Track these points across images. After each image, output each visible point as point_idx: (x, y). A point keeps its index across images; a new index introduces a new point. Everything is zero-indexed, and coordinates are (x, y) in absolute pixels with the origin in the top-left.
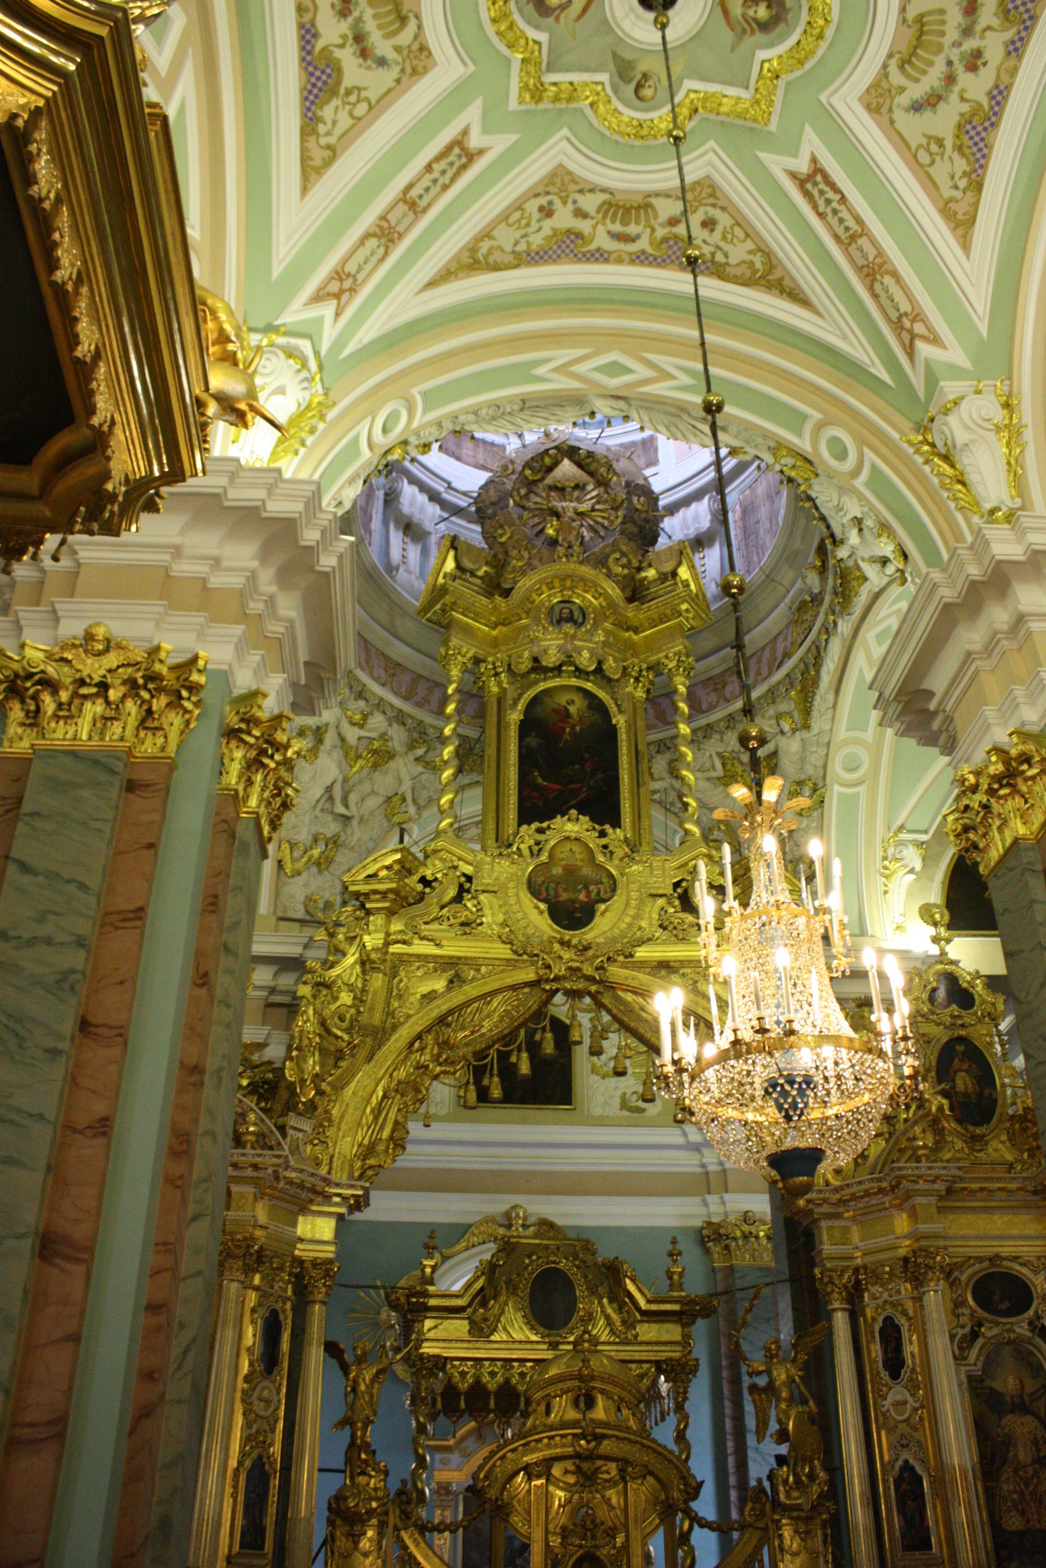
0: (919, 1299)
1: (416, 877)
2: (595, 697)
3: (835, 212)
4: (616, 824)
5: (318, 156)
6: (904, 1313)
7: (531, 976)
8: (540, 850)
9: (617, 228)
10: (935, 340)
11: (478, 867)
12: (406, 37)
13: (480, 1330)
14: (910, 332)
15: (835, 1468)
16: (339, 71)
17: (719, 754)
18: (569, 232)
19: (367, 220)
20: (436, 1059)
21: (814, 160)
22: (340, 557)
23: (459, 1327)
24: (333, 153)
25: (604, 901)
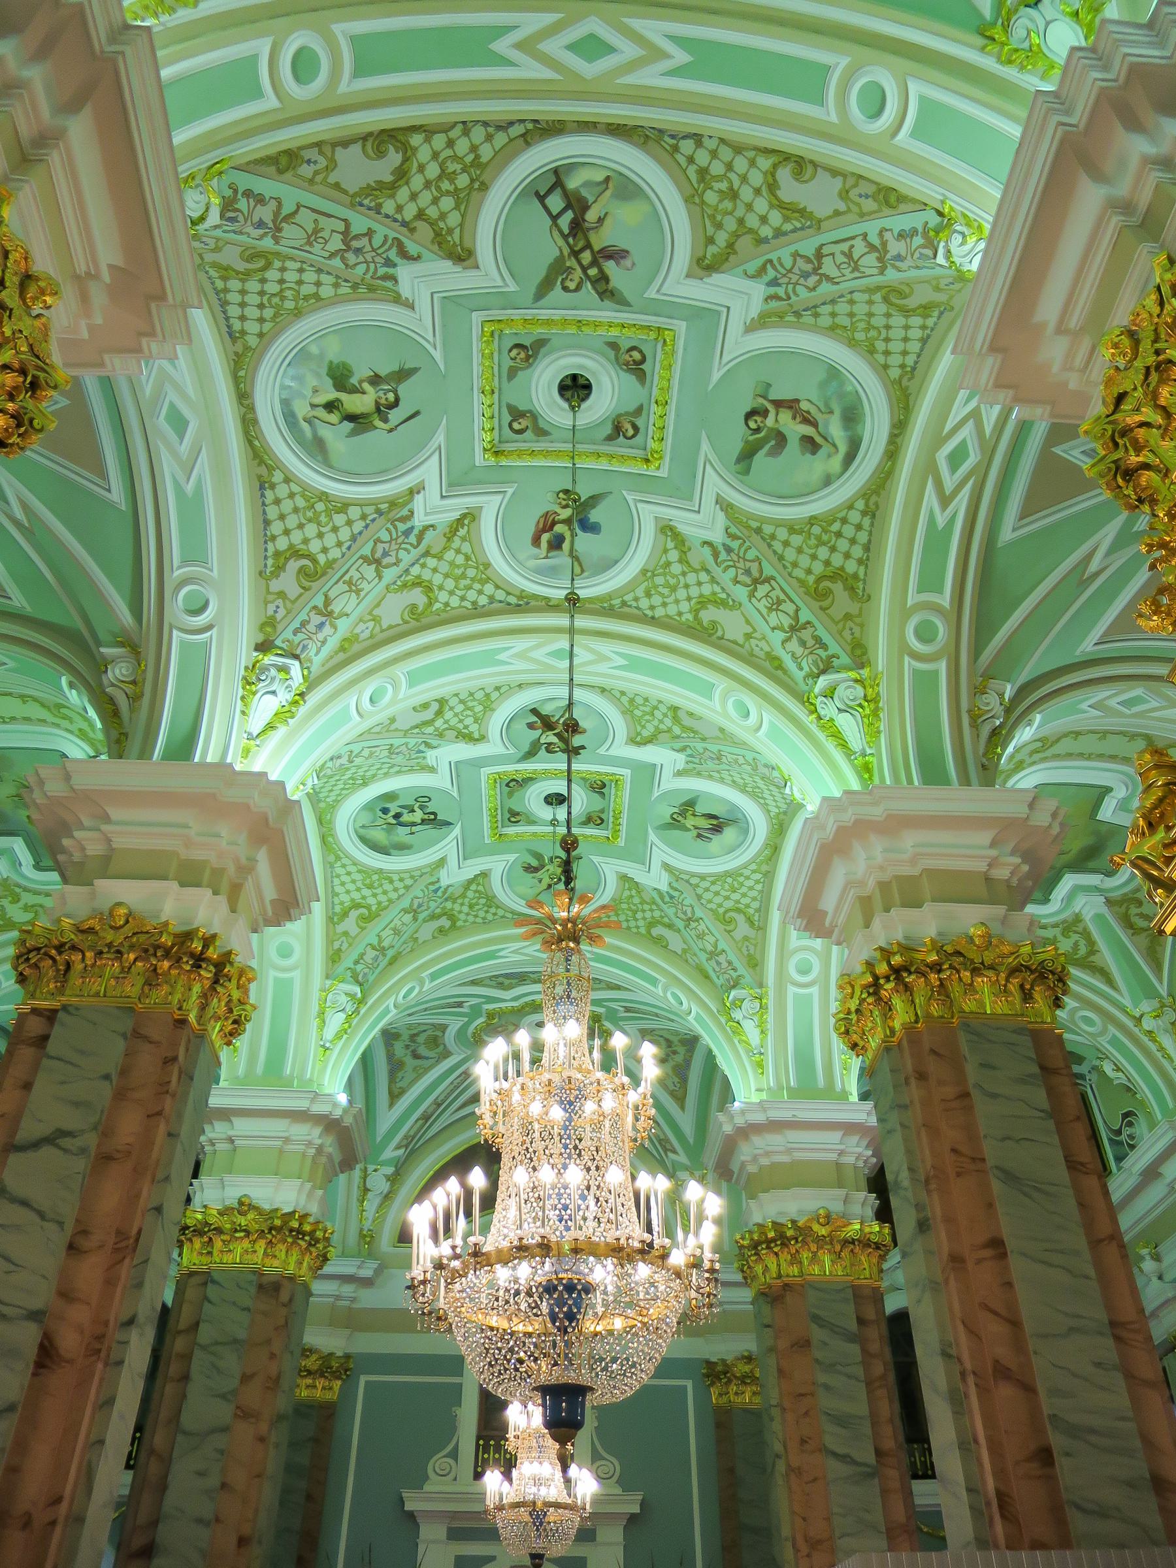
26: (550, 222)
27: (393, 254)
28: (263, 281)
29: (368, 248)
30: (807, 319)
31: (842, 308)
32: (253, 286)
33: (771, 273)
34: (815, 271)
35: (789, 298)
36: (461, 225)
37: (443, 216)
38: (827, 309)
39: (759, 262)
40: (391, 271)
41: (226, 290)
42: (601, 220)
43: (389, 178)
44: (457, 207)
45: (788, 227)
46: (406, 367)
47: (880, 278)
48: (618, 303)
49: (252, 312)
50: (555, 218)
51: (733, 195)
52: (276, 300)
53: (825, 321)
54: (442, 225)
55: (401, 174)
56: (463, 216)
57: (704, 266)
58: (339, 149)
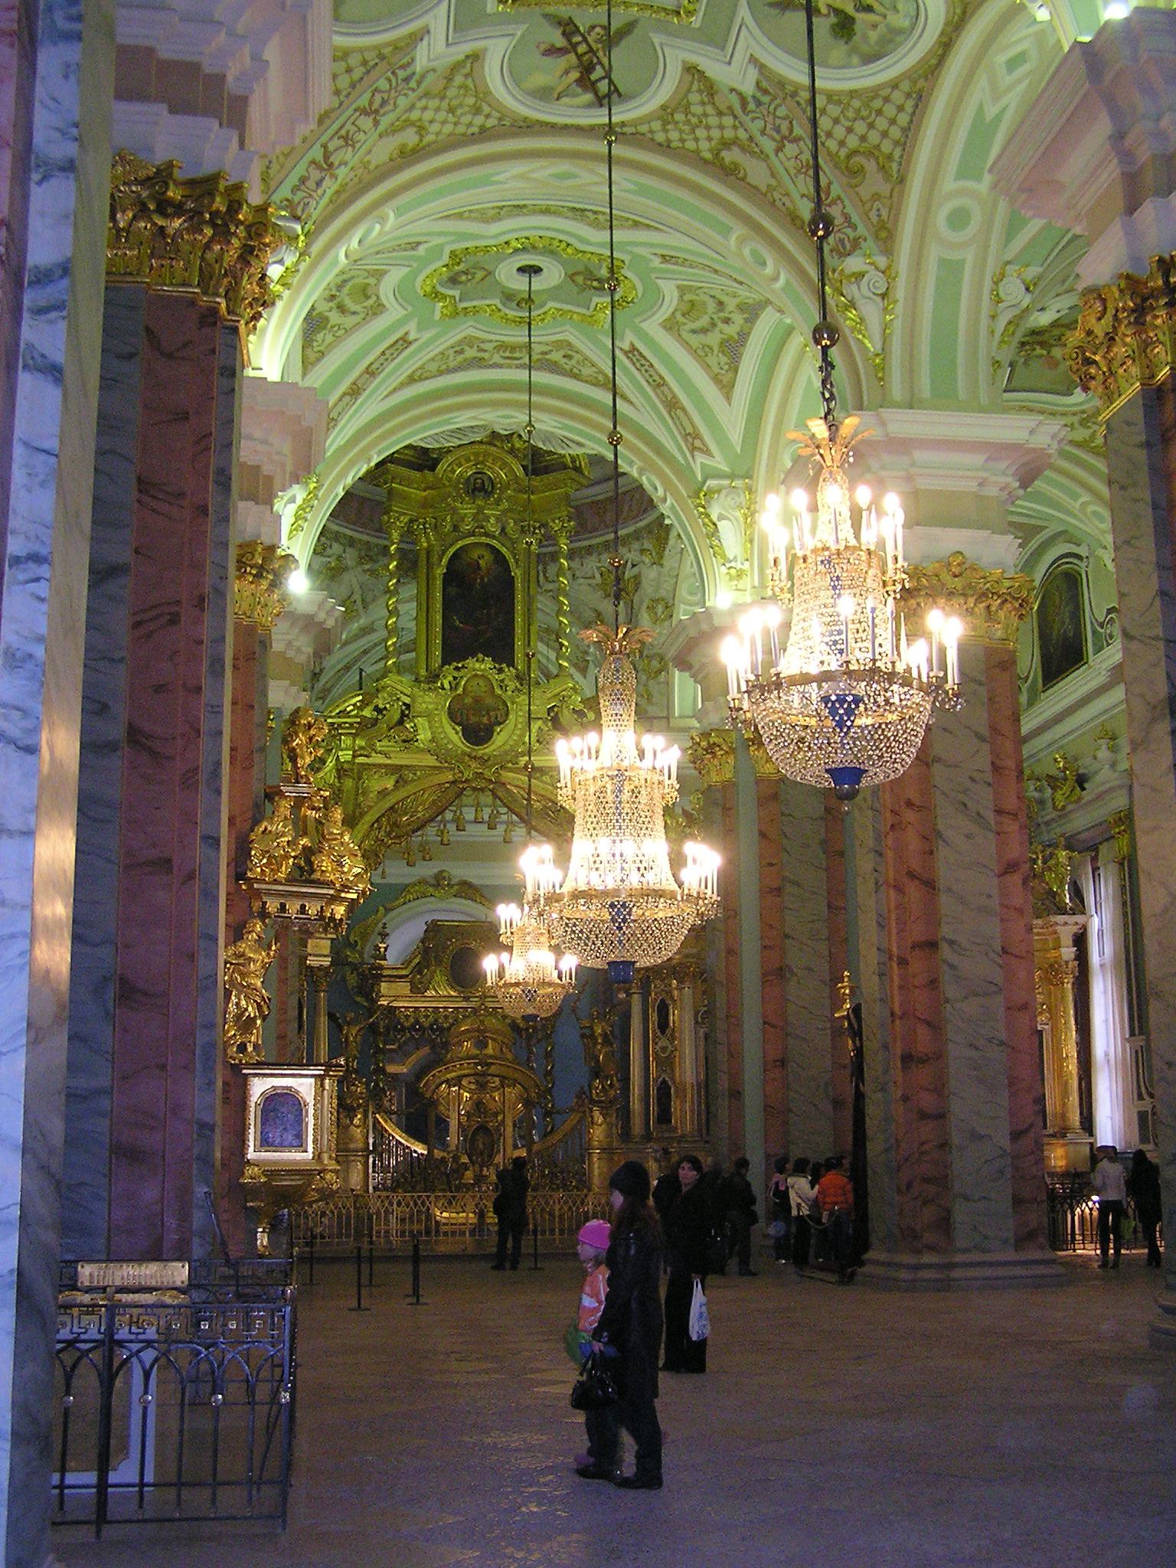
0: (680, 989)
1: (371, 707)
2: (499, 552)
3: (646, 371)
4: (511, 663)
5: (312, 357)
6: (672, 997)
7: (451, 778)
8: (457, 684)
9: (507, 354)
10: (707, 452)
11: (413, 700)
12: (371, 302)
13: (417, 989)
14: (693, 444)
15: (626, 1080)
16: (327, 319)
17: (598, 568)
18: (475, 358)
19: (344, 387)
20: (388, 834)
21: (632, 344)
22: (336, 621)
23: (404, 988)
24: (322, 354)
25: (500, 724)
26: (613, 76)
27: (752, 106)
28: (863, 138)
29: (769, 126)
30: (371, 56)
31: (344, 82)
32: (874, 137)
33: (413, 84)
34: (376, 112)
35: (393, 73)
36: (689, 90)
37: (703, 103)
38: (358, 72)
39: (423, 85)
40: (758, 95)
41: (896, 143)
42: (567, 72)
43: (736, 150)
44: (689, 104)
45: (403, 118)
46: (777, 11)
47: (324, 139)
48: (555, 16)
49: (890, 110)
50: (608, 75)
51: (451, 110)
52: (864, 113)
53: (354, 60)
54: (706, 100)
55: (726, 144)
56: (686, 96)
57: (475, 58)
58: (763, 189)
